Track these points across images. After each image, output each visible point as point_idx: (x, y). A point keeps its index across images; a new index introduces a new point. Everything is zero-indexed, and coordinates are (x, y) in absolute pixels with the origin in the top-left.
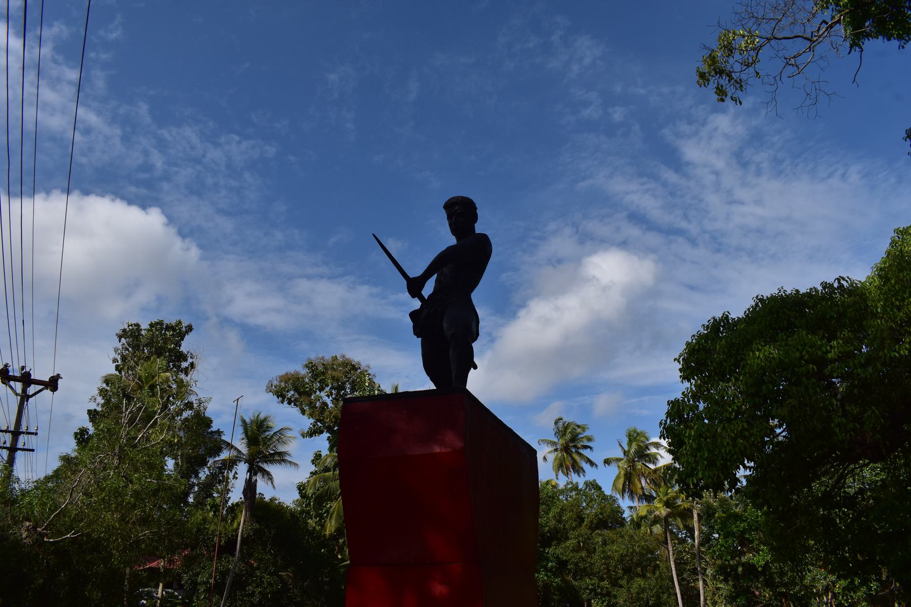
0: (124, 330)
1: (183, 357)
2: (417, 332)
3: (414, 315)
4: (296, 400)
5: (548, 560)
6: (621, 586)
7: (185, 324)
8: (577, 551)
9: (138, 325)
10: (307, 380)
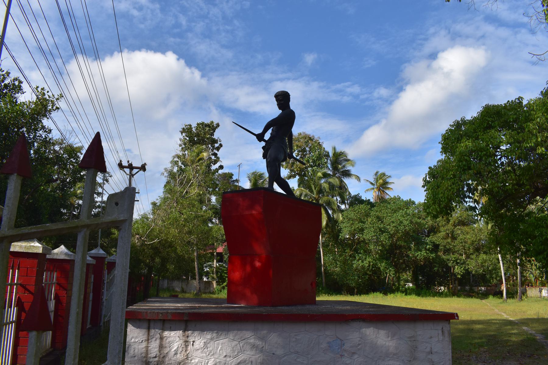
0: (183, 129)
1: (215, 141)
5: (427, 244)
6: (472, 259)
8: (445, 239)
9: (190, 125)
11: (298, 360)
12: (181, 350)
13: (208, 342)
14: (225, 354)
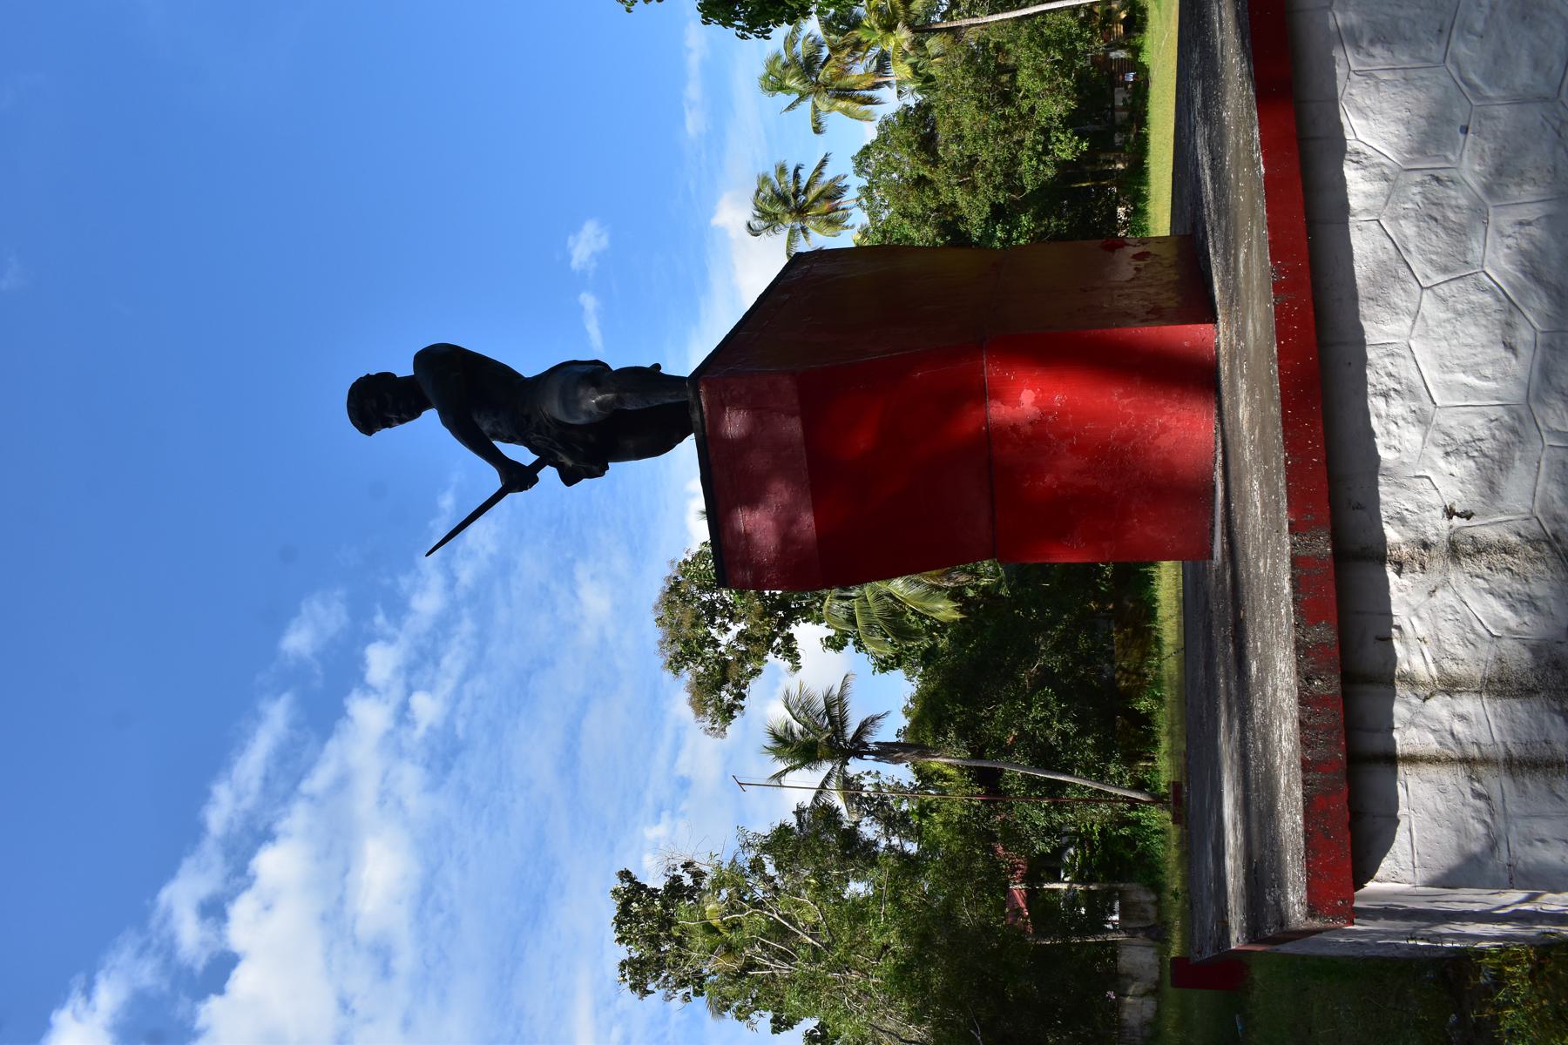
2: (598, 470)
3: (569, 478)
4: (736, 685)
7: (617, 884)
10: (701, 669)
11: (1479, 26)
12: (1505, 577)
13: (1440, 438)
14: (1501, 352)
